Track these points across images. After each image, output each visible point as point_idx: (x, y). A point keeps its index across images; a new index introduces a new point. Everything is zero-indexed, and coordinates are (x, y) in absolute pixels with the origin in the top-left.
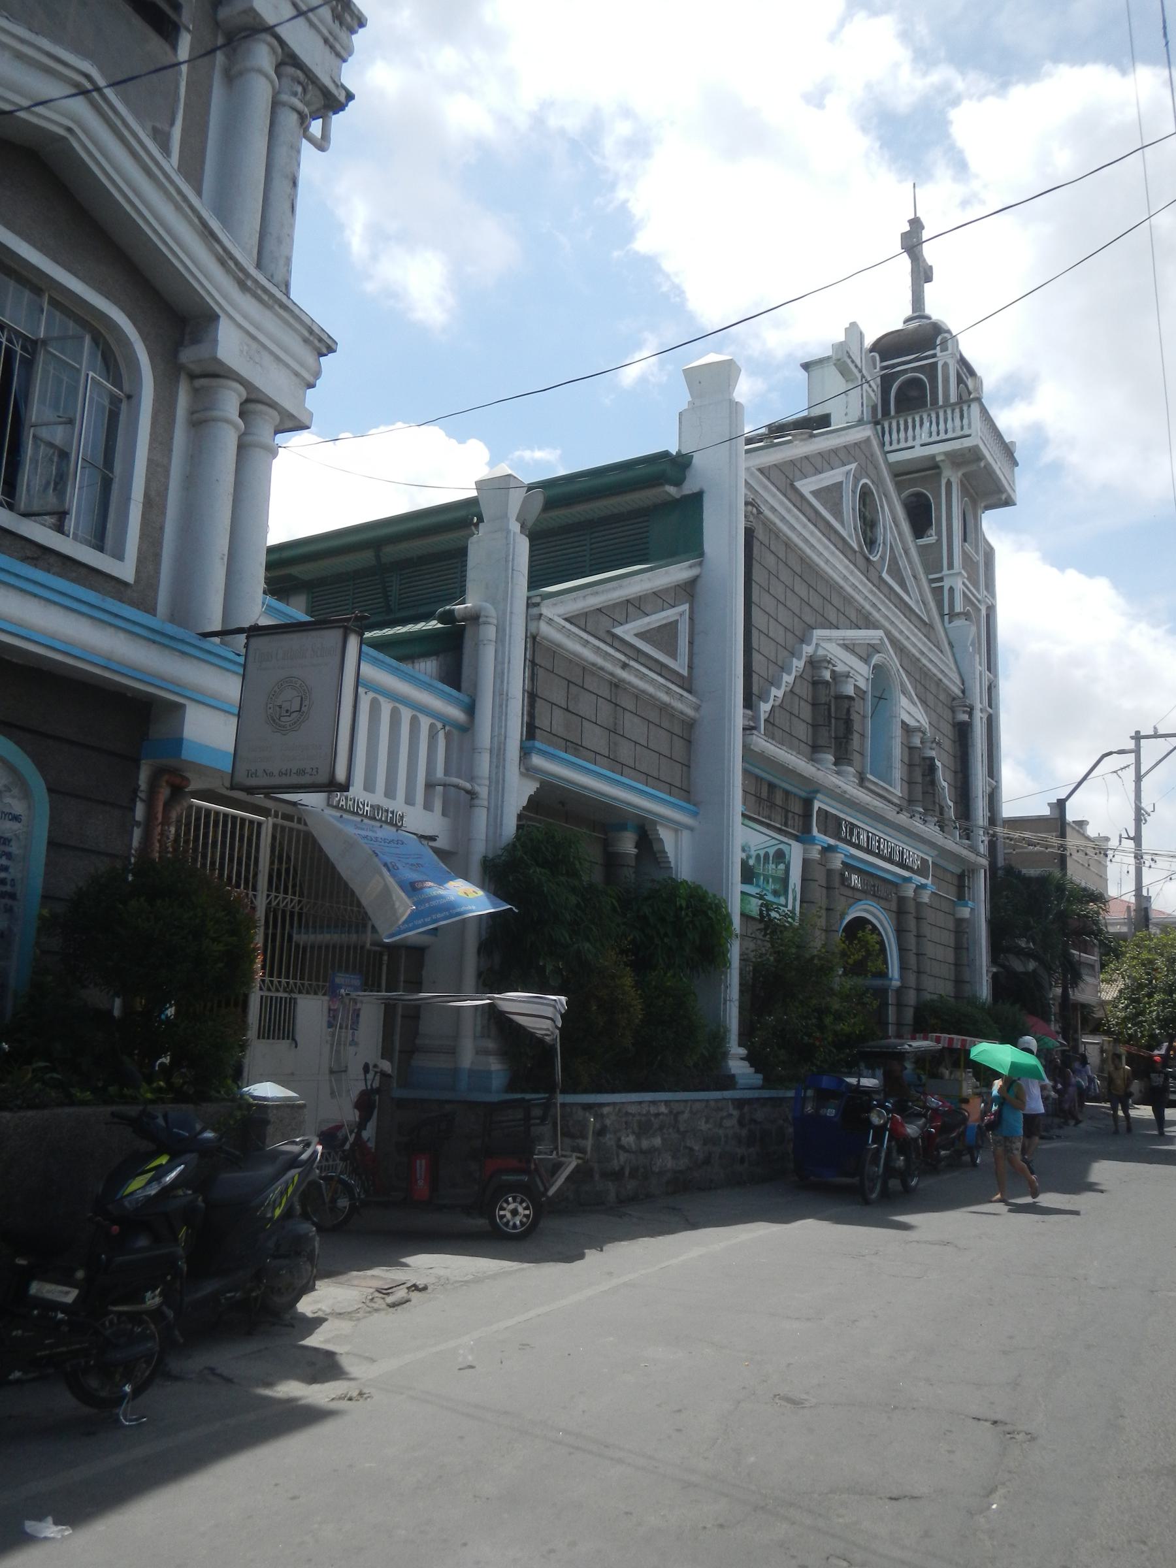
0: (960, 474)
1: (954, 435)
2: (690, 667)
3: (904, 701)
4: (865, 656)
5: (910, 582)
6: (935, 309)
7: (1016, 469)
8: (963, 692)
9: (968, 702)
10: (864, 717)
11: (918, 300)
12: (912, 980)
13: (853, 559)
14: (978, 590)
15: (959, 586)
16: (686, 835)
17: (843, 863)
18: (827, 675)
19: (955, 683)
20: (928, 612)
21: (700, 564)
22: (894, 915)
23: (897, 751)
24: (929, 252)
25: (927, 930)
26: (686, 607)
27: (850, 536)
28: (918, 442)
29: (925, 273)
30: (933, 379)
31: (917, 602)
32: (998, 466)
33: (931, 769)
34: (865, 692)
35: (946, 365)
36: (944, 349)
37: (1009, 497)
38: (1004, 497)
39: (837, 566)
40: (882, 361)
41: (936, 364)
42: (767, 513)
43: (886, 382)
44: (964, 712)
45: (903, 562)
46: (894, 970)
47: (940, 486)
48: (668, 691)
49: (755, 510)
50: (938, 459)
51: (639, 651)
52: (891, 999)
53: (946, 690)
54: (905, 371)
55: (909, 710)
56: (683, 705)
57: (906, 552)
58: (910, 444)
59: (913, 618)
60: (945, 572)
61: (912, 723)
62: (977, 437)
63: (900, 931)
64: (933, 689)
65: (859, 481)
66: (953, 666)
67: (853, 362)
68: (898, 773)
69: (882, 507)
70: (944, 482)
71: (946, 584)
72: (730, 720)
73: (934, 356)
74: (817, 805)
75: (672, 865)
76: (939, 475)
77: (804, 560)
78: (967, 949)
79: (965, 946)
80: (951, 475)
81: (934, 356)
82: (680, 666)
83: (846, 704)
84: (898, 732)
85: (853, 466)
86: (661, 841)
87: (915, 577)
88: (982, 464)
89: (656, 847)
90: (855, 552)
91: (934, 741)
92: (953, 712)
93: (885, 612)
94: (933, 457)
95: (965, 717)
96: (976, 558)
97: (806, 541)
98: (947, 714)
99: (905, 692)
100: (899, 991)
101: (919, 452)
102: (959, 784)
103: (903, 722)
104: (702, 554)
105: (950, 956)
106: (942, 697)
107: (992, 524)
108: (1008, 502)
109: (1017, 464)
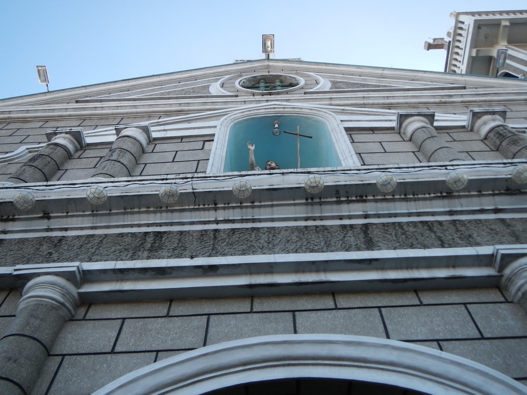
50: (474, 54)
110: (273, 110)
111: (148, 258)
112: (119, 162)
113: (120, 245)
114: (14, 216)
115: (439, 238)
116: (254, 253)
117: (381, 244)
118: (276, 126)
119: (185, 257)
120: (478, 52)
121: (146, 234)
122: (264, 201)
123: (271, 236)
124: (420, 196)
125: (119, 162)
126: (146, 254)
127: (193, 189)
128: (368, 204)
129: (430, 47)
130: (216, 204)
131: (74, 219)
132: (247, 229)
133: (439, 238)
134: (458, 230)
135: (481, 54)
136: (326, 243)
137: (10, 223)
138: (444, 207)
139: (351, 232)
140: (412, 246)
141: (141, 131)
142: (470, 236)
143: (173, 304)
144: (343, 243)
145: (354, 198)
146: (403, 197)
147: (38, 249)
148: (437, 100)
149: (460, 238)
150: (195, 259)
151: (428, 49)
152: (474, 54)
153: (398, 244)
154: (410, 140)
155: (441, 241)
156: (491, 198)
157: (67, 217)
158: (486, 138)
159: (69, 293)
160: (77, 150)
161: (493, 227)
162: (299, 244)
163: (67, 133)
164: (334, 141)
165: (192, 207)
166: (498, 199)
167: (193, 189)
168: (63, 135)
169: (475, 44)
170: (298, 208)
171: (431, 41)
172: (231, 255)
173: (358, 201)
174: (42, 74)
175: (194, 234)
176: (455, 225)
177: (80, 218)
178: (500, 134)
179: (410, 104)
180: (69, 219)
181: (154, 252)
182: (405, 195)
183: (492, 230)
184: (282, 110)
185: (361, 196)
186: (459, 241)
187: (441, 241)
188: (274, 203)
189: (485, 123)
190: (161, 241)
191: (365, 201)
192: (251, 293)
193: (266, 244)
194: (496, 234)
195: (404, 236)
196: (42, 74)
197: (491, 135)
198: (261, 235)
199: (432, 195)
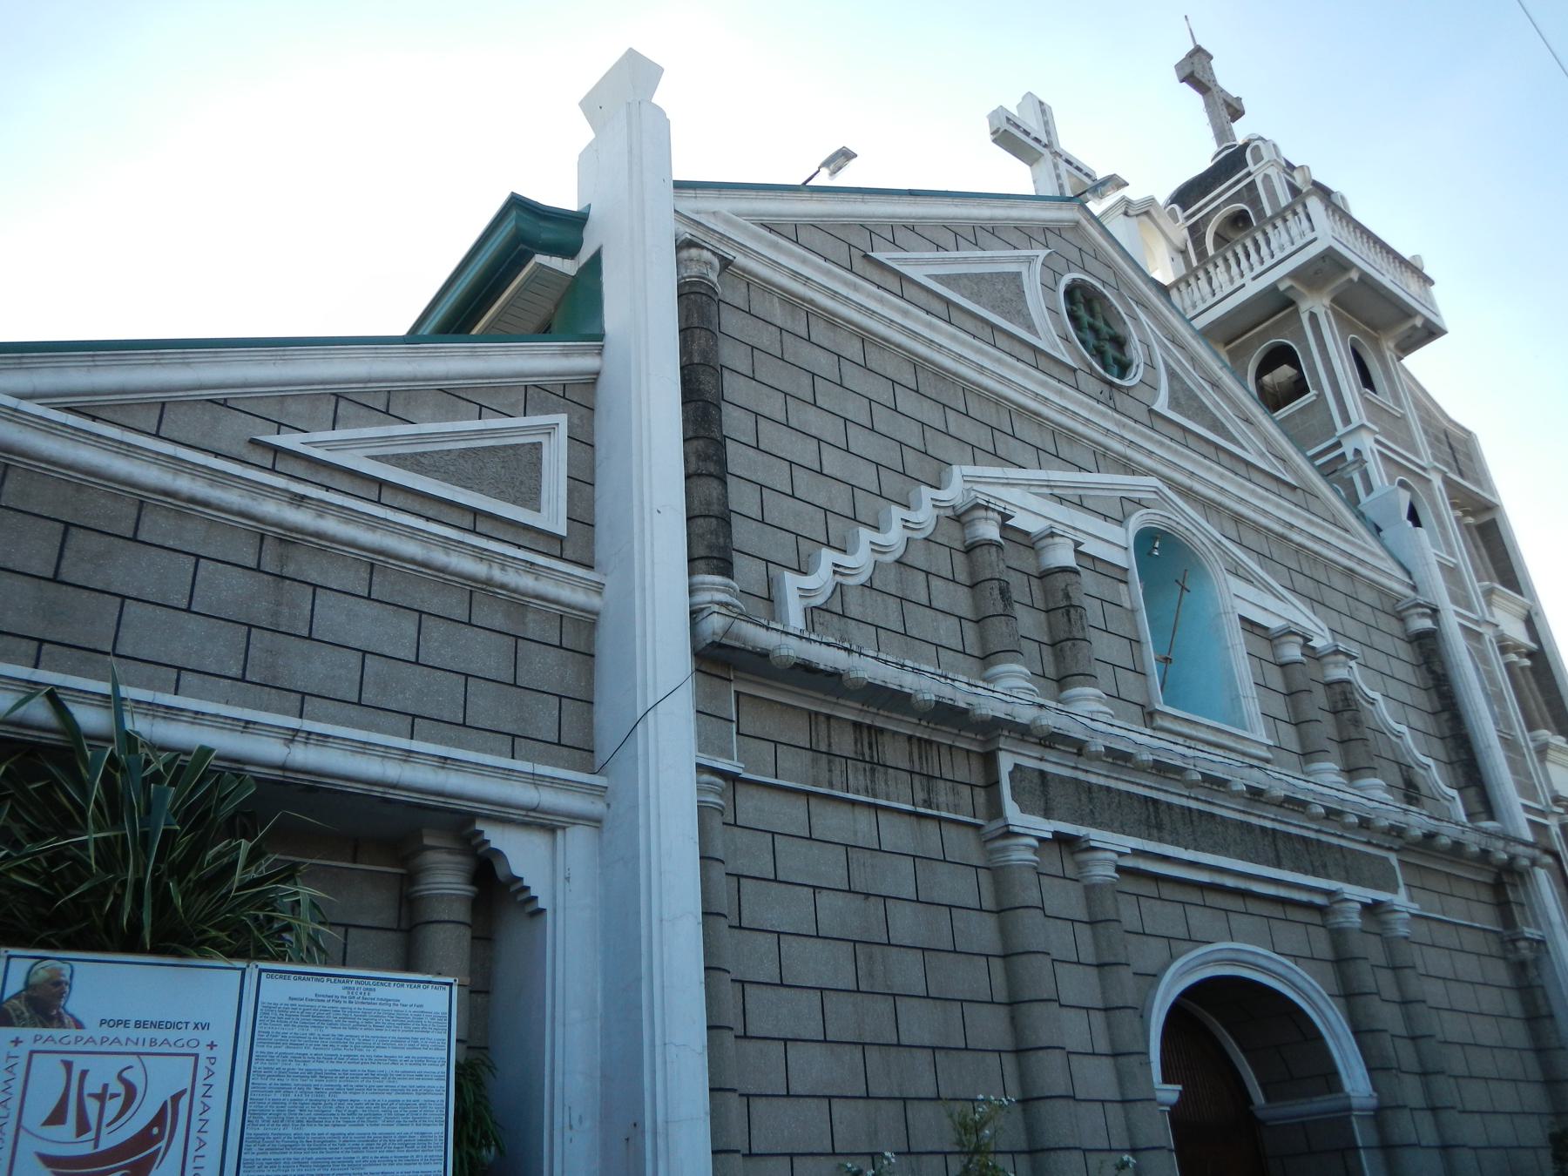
0: (1327, 301)
1: (1294, 248)
2: (582, 519)
3: (1237, 585)
4: (1119, 516)
5: (1235, 426)
6: (1241, 131)
7: (1433, 289)
8: (1414, 588)
9: (1421, 600)
10: (1133, 611)
11: (1222, 134)
12: (1411, 1091)
13: (1072, 382)
14: (1417, 454)
15: (1367, 443)
16: (577, 840)
17: (1119, 869)
18: (991, 531)
19: (1390, 576)
20: (1296, 472)
21: (600, 352)
22: (1329, 968)
23: (1243, 669)
24: (1227, 77)
25: (1434, 992)
26: (562, 419)
27: (1055, 346)
28: (1249, 275)
29: (1228, 105)
30: (1255, 201)
31: (1262, 455)
32: (1388, 278)
33: (1343, 700)
34: (1126, 570)
35: (1267, 177)
36: (1258, 158)
37: (1427, 321)
38: (1418, 322)
39: (1021, 383)
40: (1185, 209)
41: (1253, 184)
42: (741, 260)
43: (1196, 232)
44: (1424, 615)
45: (1209, 398)
46: (1356, 1082)
47: (1302, 327)
48: (481, 554)
49: (707, 255)
50: (1282, 287)
51: (382, 483)
52: (1362, 1134)
53: (1373, 585)
54: (1217, 209)
55: (1243, 597)
56: (562, 585)
57: (1215, 385)
58: (1237, 284)
59: (1256, 476)
60: (1341, 429)
61: (1274, 624)
62: (1326, 233)
63: (1349, 996)
64: (1339, 582)
65: (1057, 276)
66: (1382, 553)
67: (1027, 134)
68: (1251, 705)
69: (1135, 318)
70: (1305, 318)
71: (1348, 448)
72: (643, 589)
73: (1249, 174)
74: (1006, 763)
75: (542, 903)
76: (1297, 311)
77: (918, 364)
78: (1551, 1016)
79: (1544, 1011)
80: (1316, 305)
81: (1249, 174)
82: (553, 515)
83: (1061, 580)
84: (1237, 639)
85: (1042, 253)
86: (498, 853)
87: (1247, 421)
88: (1354, 275)
89: (500, 872)
90: (1074, 370)
91: (1337, 652)
92: (1402, 620)
93: (1158, 450)
94: (1273, 288)
95: (1427, 624)
96: (1397, 412)
97: (915, 335)
98: (1395, 626)
99: (1236, 571)
100: (1380, 1115)
101: (1253, 288)
102: (1447, 733)
103: (1242, 618)
104: (600, 337)
105: (1518, 1034)
106: (1368, 596)
107: (1421, 364)
108: (1432, 332)
109: (1432, 283)
120: (1291, 287)
152: (1282, 287)
189: (1336, 664)
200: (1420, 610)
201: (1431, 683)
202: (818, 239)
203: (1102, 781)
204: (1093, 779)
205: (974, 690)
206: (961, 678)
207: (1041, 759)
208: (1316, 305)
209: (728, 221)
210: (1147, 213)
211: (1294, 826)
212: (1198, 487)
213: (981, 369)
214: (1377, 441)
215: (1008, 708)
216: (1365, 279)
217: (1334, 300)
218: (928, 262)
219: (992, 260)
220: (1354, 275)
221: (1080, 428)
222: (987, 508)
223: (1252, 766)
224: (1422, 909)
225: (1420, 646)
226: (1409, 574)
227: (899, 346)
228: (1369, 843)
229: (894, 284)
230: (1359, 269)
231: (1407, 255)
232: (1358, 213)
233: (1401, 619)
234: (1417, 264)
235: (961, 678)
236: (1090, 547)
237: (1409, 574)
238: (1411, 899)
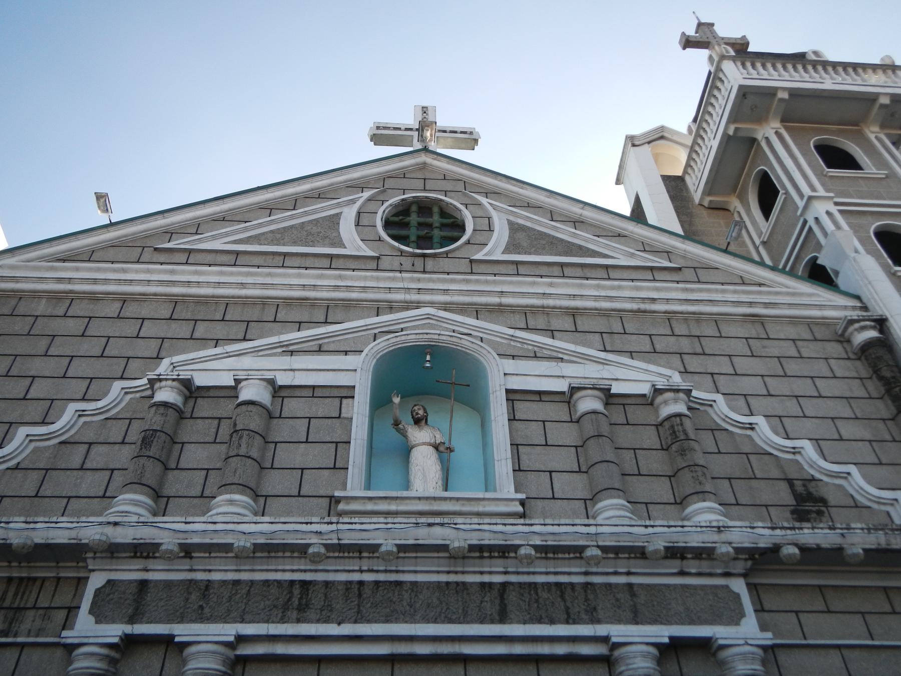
31: (632, 255)
44: (864, 328)
61: (565, 388)
80: (769, 131)
98: (835, 349)
101: (715, 144)
110: (425, 336)
111: (298, 621)
112: (249, 457)
113: (269, 600)
114: (154, 553)
115: (567, 609)
116: (397, 621)
117: (512, 616)
118: (428, 358)
119: (332, 622)
120: (736, 129)
121: (292, 582)
122: (409, 552)
123: (413, 595)
124: (560, 556)
125: (249, 457)
126: (294, 614)
127: (339, 539)
128: (509, 561)
129: (688, 43)
130: (360, 553)
131: (218, 560)
132: (391, 582)
133: (567, 609)
134: (586, 600)
135: (740, 134)
136: (463, 610)
137: (151, 560)
138: (581, 567)
139: (488, 594)
140: (540, 621)
141: (265, 384)
142: (595, 609)
143: (322, 666)
144: (480, 610)
145: (496, 554)
146: (543, 555)
147: (187, 599)
148: (635, 306)
149: (586, 611)
150: (342, 625)
151: (684, 48)
152: (731, 132)
153: (528, 616)
154: (578, 422)
155: (568, 614)
156: (625, 561)
157: (210, 557)
158: (661, 424)
159: (228, 658)
160: (186, 399)
161: (619, 596)
162: (439, 610)
163: (174, 380)
164: (493, 418)
165: (336, 554)
166: (632, 561)
167: (339, 539)
168: (169, 383)
169: (734, 117)
170: (442, 561)
171: (691, 32)
172: (376, 622)
173: (499, 557)
174: (102, 199)
175: (340, 588)
176: (585, 591)
177: (223, 559)
178: (674, 432)
179: (601, 310)
180: (212, 560)
181: (302, 613)
182: (546, 553)
183: (617, 600)
184: (436, 337)
185: (504, 553)
186: (584, 616)
187: (568, 614)
188: (419, 555)
189: (666, 402)
190: (308, 595)
191: (507, 558)
192: (392, 660)
193: (408, 608)
194: (619, 607)
195: (536, 605)
196: (102, 199)
197: (667, 425)
198: (404, 593)
199: (572, 555)
200: (857, 325)
201: (883, 390)
202: (111, 254)
203: (230, 576)
204: (216, 576)
205: (32, 526)
206: (16, 519)
207: (191, 570)
208: (769, 131)
209: (26, 268)
210: (662, 138)
211: (571, 574)
212: (506, 300)
213: (243, 285)
214: (836, 204)
215: (73, 534)
216: (796, 94)
217: (783, 121)
218: (227, 234)
219: (306, 213)
220: (785, 95)
221: (354, 295)
222: (160, 380)
223: (430, 525)
224: (776, 636)
225: (867, 359)
226: (858, 298)
227: (155, 295)
228: (682, 573)
229: (183, 258)
230: (784, 89)
231: (877, 61)
232: (832, 56)
233: (843, 339)
234: (888, 62)
235: (16, 519)
236: (283, 379)
237: (858, 298)
238: (763, 627)
